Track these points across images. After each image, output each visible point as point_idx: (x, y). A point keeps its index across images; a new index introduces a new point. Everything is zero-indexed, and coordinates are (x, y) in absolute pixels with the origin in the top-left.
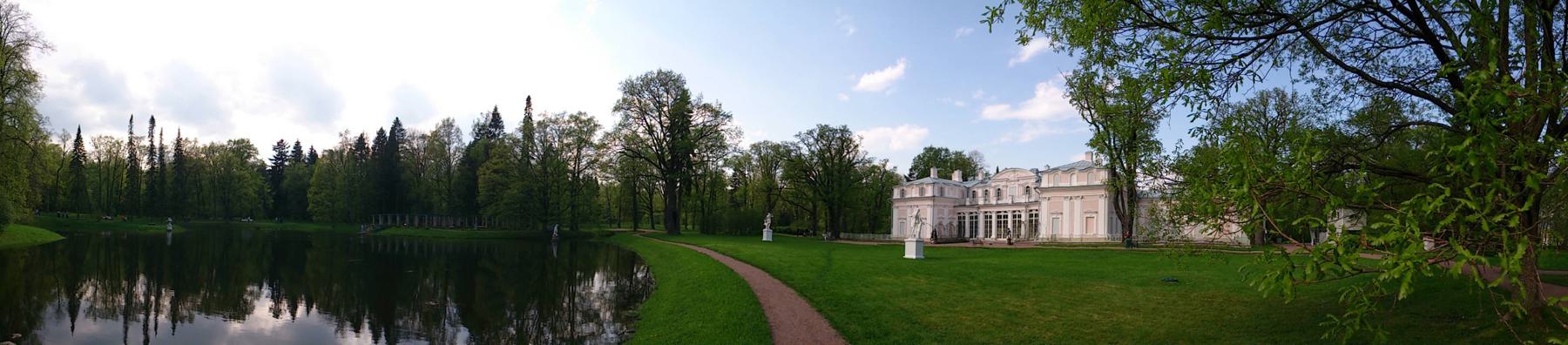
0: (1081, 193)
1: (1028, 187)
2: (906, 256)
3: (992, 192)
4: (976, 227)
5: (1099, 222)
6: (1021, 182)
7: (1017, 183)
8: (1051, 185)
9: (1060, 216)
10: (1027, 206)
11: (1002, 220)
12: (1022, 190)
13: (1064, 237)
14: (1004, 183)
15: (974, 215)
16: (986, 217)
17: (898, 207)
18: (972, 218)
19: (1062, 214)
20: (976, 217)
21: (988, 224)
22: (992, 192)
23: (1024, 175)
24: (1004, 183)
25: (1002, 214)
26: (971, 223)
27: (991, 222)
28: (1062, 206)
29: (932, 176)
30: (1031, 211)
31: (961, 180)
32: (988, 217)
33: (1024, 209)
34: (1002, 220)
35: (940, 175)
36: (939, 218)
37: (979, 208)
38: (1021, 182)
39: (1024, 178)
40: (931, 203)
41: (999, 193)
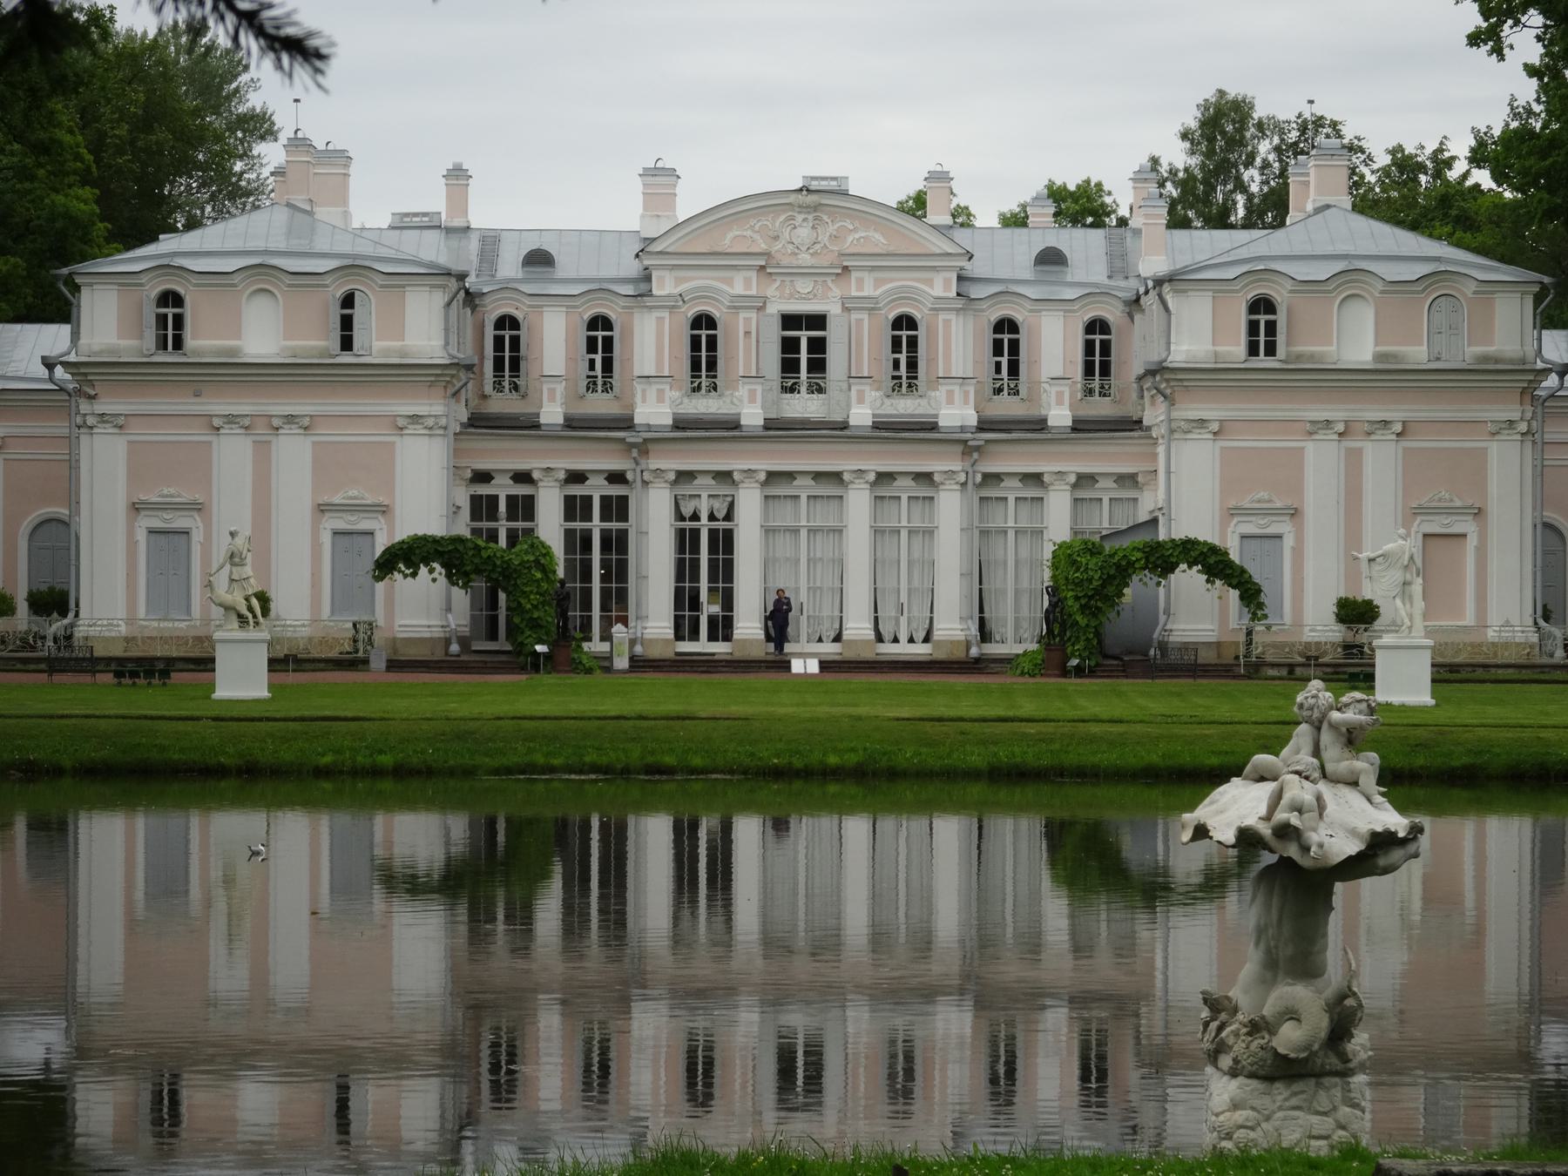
0: (1397, 413)
1: (905, 322)
2: (1381, 695)
4: (617, 572)
5: (1494, 566)
6: (866, 286)
7: (836, 291)
9: (1284, 527)
10: (967, 449)
13: (1309, 636)
14: (741, 284)
15: (597, 489)
17: (118, 423)
18: (575, 508)
19: (1295, 513)
20: (617, 508)
23: (878, 240)
24: (741, 284)
28: (1300, 467)
30: (992, 478)
33: (956, 466)
37: (644, 448)
38: (866, 286)
39: (880, 263)
40: (433, 406)
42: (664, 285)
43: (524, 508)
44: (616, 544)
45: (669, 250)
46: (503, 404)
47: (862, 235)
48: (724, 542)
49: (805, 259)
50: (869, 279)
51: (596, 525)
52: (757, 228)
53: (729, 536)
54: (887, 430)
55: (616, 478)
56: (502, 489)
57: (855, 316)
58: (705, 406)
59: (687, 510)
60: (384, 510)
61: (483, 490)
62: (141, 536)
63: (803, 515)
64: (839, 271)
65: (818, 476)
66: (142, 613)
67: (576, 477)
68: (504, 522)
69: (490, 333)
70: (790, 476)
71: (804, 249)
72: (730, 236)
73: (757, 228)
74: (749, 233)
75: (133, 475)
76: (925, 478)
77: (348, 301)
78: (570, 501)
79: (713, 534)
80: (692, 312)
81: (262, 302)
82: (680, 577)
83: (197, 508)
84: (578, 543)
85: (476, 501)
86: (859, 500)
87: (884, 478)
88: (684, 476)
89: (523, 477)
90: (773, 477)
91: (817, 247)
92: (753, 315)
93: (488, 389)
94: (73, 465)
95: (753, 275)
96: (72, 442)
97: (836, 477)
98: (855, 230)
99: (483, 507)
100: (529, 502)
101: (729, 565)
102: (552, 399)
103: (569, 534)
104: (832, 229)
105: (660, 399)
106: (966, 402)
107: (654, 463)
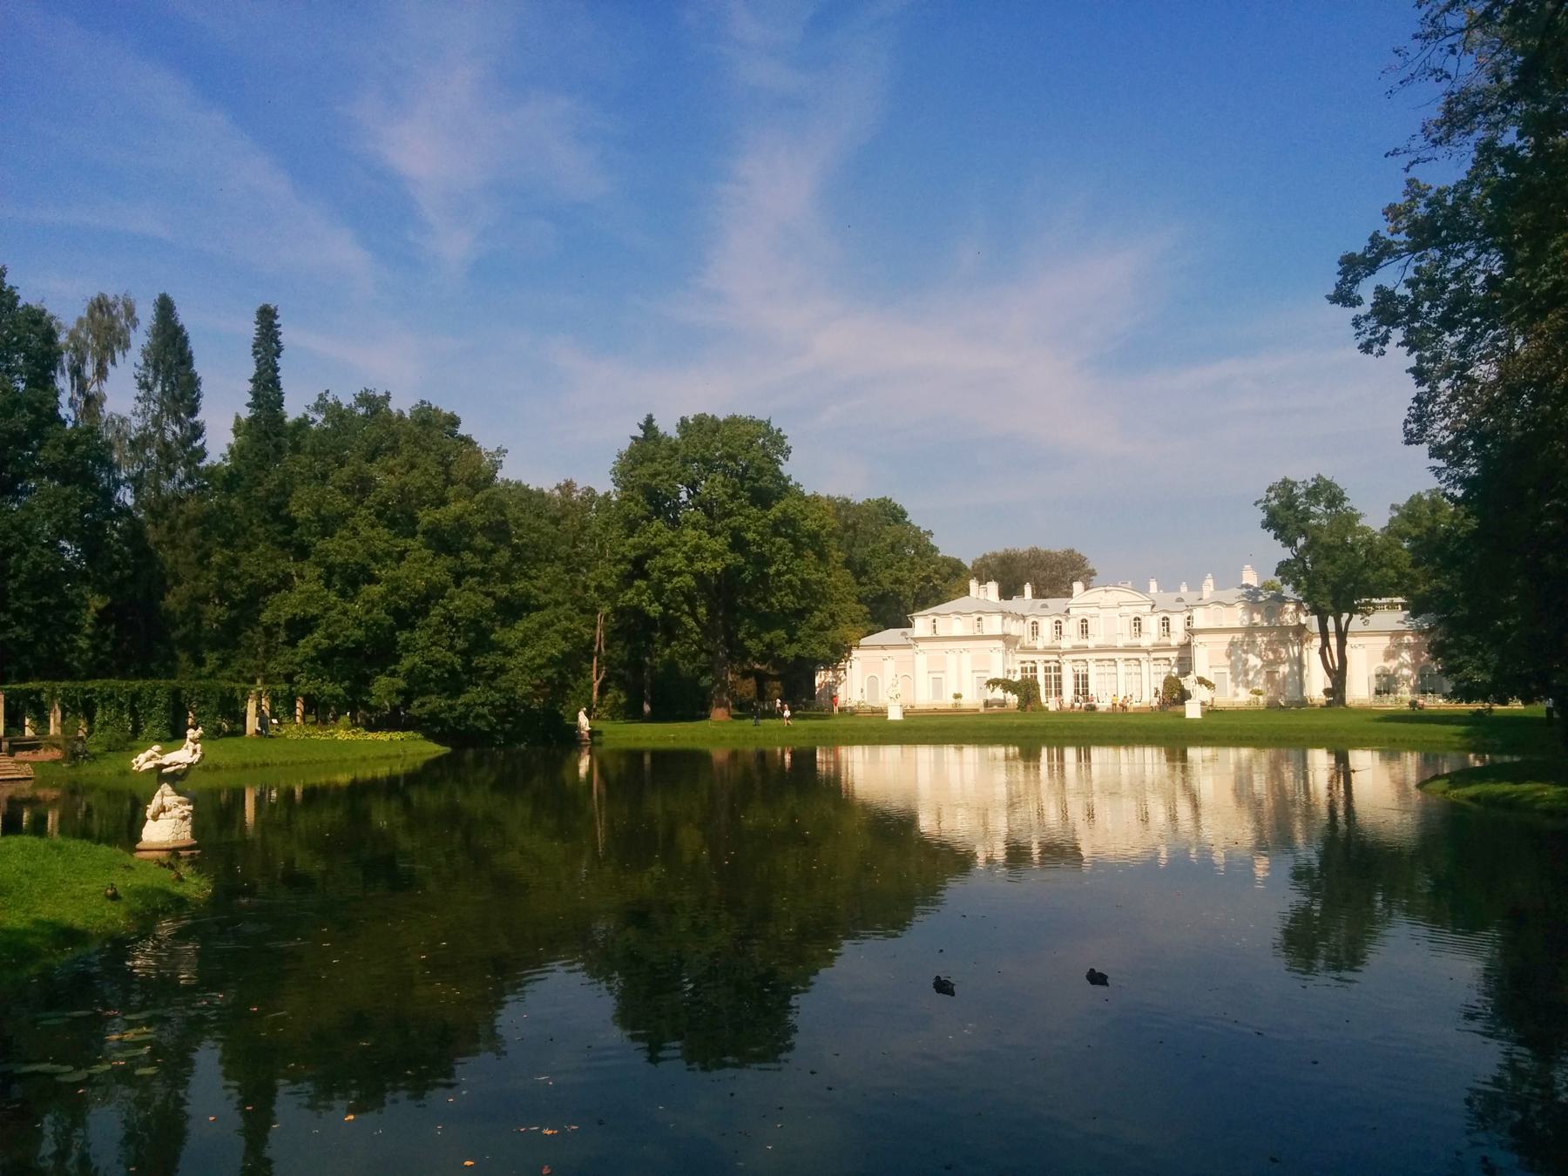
2: (1188, 716)
3: (1071, 627)
6: (1125, 610)
7: (1118, 611)
8: (1211, 625)
10: (1148, 652)
12: (1125, 625)
15: (1053, 665)
18: (1047, 670)
20: (1059, 669)
22: (1071, 627)
30: (1155, 659)
37: (1064, 654)
41: (1084, 628)
42: (1072, 611)
43: (1034, 670)
44: (1059, 678)
46: (1033, 644)
48: (1085, 677)
51: (1053, 674)
53: (1087, 676)
54: (1128, 649)
55: (1057, 661)
56: (1029, 665)
58: (1084, 642)
59: (1076, 669)
60: (987, 671)
61: (1024, 665)
62: (931, 680)
63: (1108, 670)
65: (1109, 660)
66: (931, 697)
67: (1047, 662)
69: (1031, 626)
70: (1102, 660)
76: (1137, 659)
78: (1046, 668)
80: (1082, 618)
83: (943, 672)
84: (1048, 678)
85: (1022, 668)
86: (1121, 665)
87: (1127, 660)
88: (1074, 661)
89: (1033, 662)
90: (1097, 660)
93: (1031, 639)
94: (913, 661)
96: (913, 656)
97: (1113, 660)
99: (1024, 670)
100: (1035, 668)
101: (1087, 683)
103: (1046, 676)
107: (1066, 657)
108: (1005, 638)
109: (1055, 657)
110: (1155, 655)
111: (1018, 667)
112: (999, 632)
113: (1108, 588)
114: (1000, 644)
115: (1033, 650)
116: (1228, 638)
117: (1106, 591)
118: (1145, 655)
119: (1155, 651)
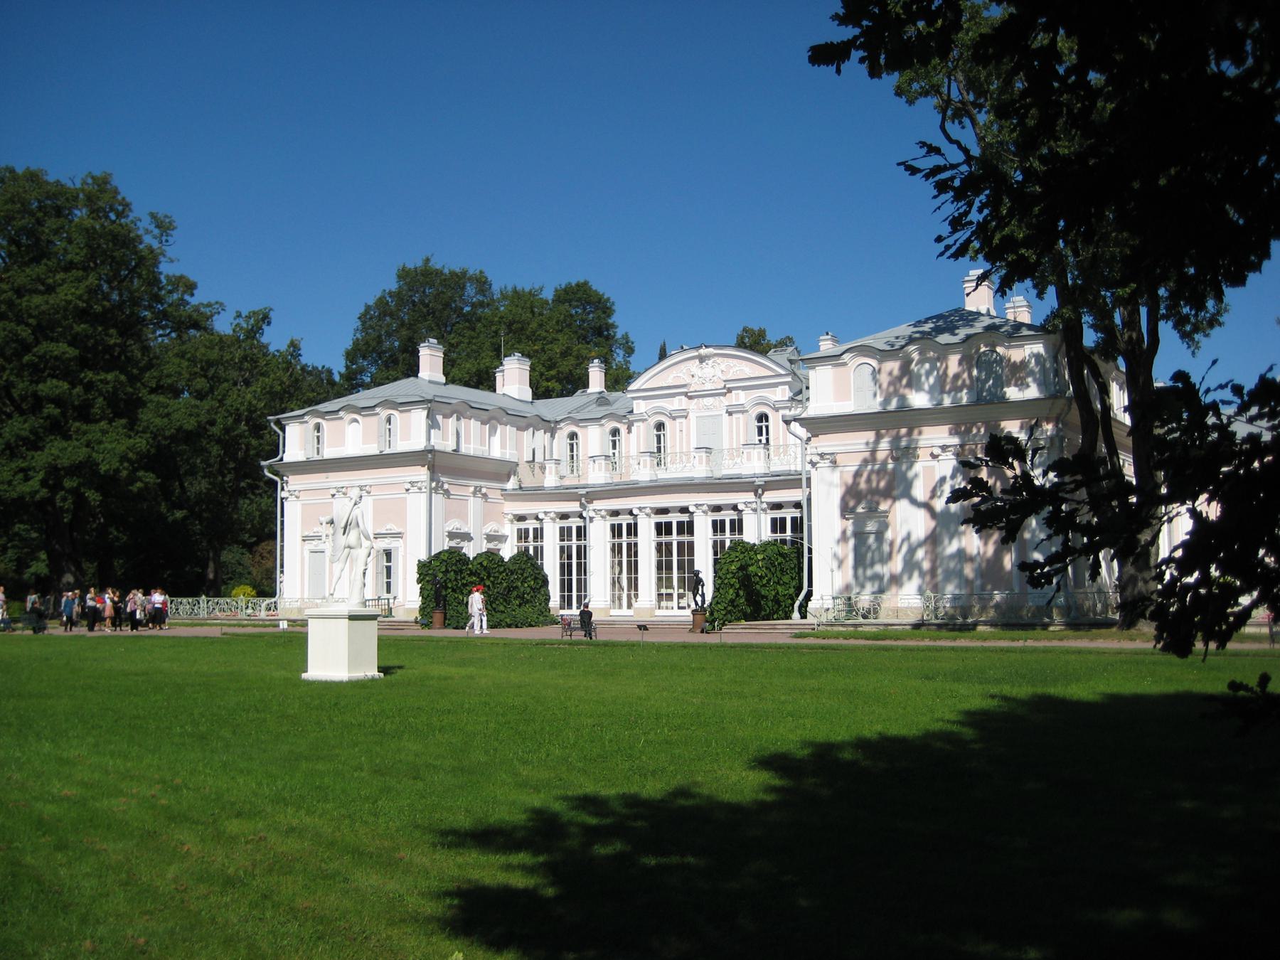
4: (582, 569)
6: (740, 397)
11: (675, 538)
15: (574, 523)
16: (616, 531)
18: (565, 533)
20: (581, 533)
21: (625, 555)
24: (677, 403)
25: (674, 518)
26: (565, 552)
27: (633, 550)
29: (424, 373)
30: (777, 506)
31: (527, 394)
32: (624, 532)
34: (675, 538)
35: (452, 372)
36: (452, 536)
43: (539, 534)
44: (582, 552)
45: (642, 388)
47: (737, 369)
49: (708, 386)
50: (741, 393)
51: (574, 542)
52: (684, 371)
57: (735, 416)
62: (307, 554)
64: (725, 391)
67: (564, 516)
68: (532, 543)
70: (664, 511)
71: (707, 380)
72: (672, 376)
73: (684, 371)
74: (681, 375)
75: (305, 523)
77: (389, 421)
79: (629, 545)
81: (355, 424)
82: (562, 574)
91: (715, 378)
92: (683, 420)
95: (683, 397)
98: (735, 365)
99: (523, 535)
102: (550, 473)
104: (723, 367)
105: (600, 470)
106: (759, 459)
107: (598, 504)
108: (430, 459)
109: (573, 507)
110: (772, 496)
111: (510, 530)
112: (418, 443)
113: (703, 351)
114: (421, 474)
115: (538, 494)
116: (858, 441)
117: (702, 359)
118: (750, 497)
119: (768, 486)
